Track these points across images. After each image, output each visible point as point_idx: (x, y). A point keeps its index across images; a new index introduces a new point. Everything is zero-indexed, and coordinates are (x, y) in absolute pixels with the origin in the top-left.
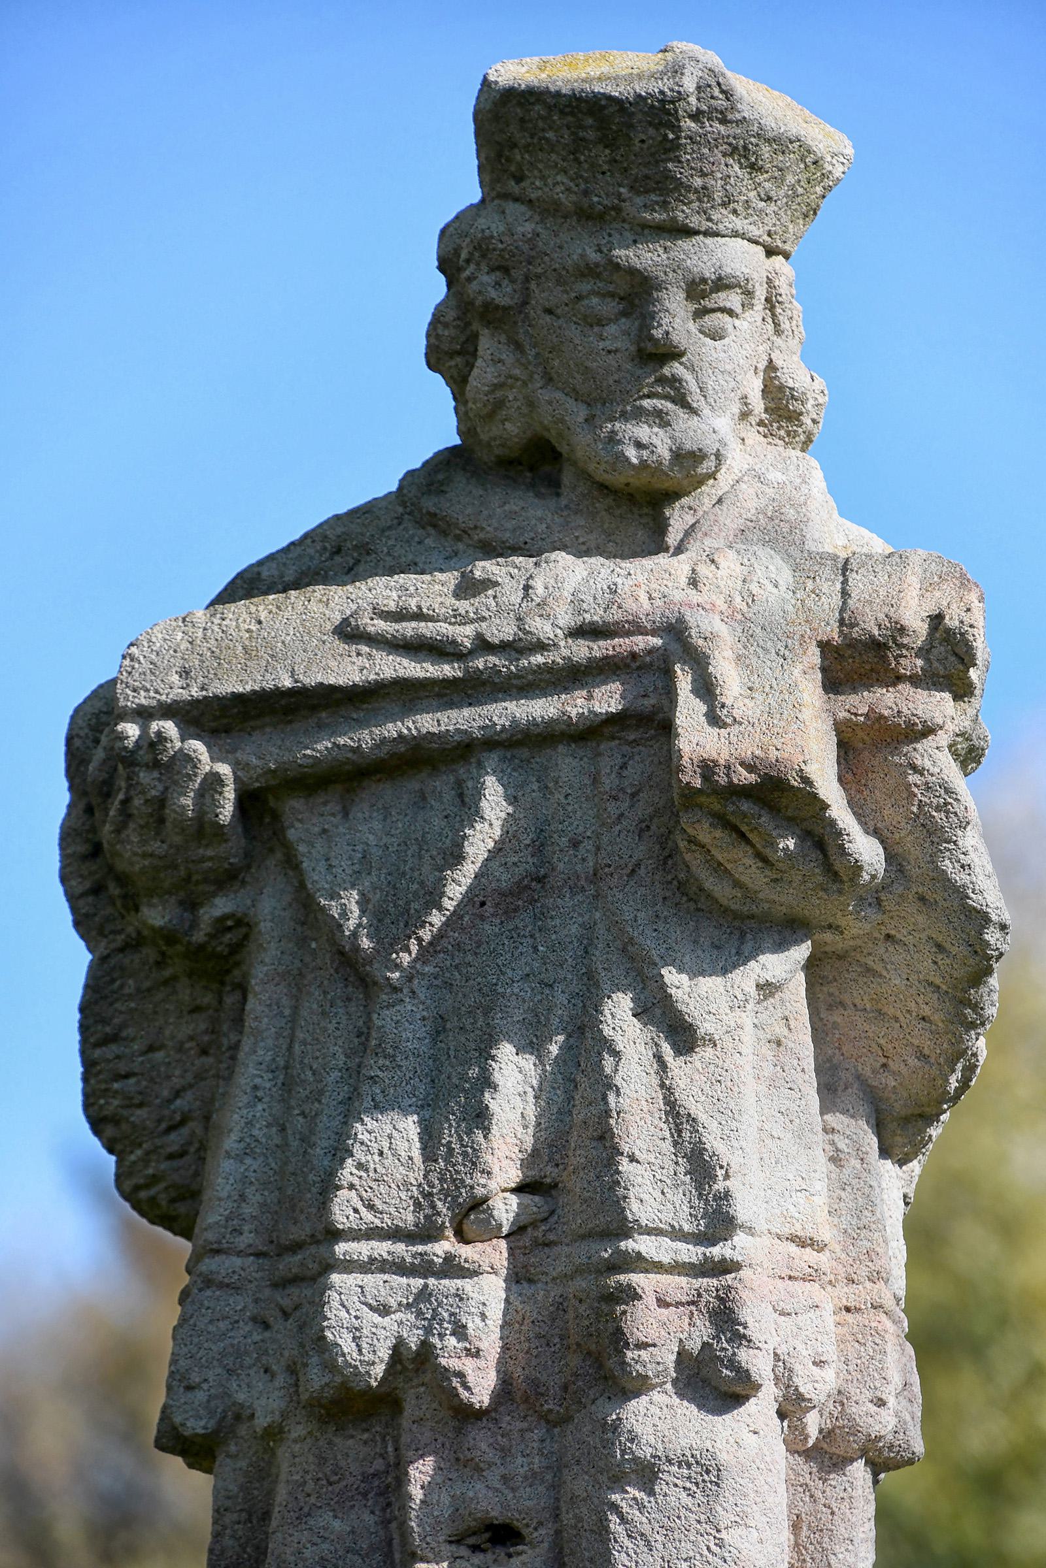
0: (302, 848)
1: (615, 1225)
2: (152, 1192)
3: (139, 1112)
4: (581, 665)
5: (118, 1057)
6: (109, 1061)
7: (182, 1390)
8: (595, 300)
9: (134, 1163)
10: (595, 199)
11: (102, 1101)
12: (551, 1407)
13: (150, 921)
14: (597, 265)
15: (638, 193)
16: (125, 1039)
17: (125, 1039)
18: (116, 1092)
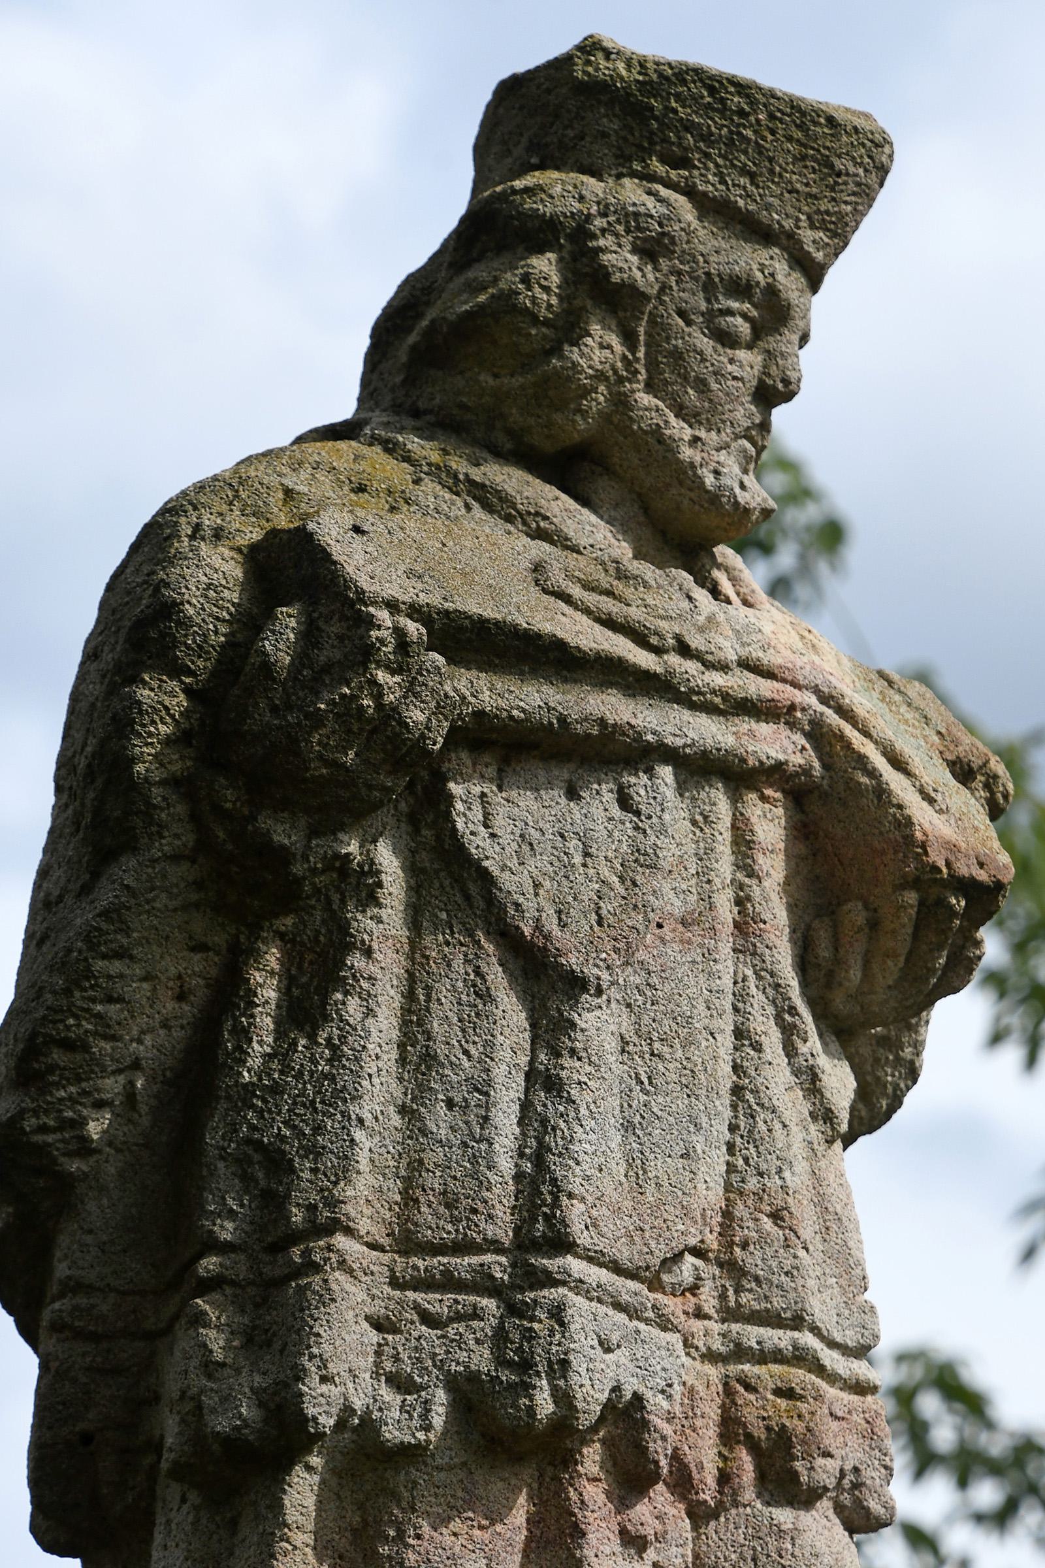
0: (459, 806)
1: (788, 1315)
2: (50, 1138)
3: (103, 1044)
4: (751, 701)
5: (121, 976)
6: (110, 977)
7: (318, 1378)
8: (739, 320)
9: (61, 1100)
10: (776, 216)
11: (71, 1021)
12: (708, 1498)
13: (276, 838)
14: (758, 283)
15: (812, 226)
16: (131, 957)
17: (131, 957)
18: (99, 1016)
